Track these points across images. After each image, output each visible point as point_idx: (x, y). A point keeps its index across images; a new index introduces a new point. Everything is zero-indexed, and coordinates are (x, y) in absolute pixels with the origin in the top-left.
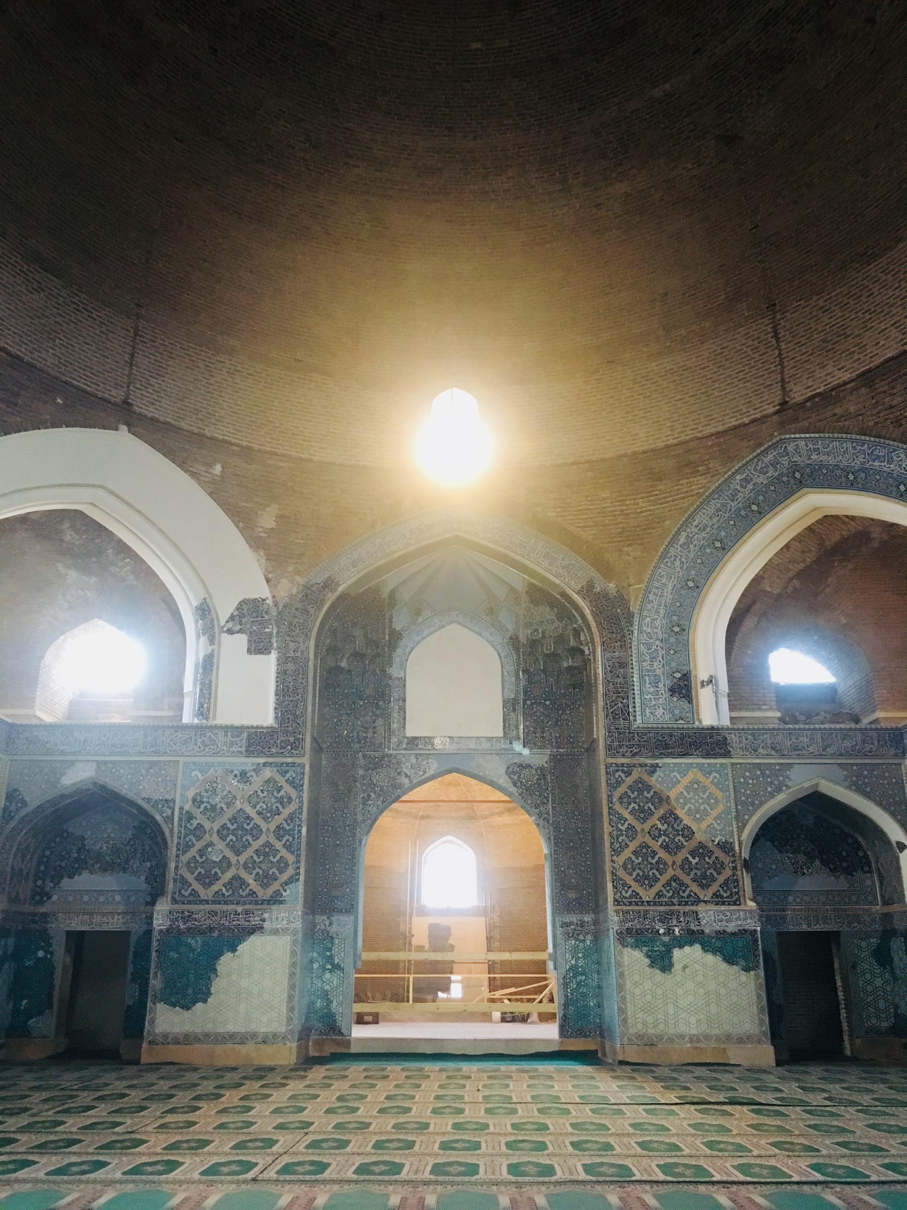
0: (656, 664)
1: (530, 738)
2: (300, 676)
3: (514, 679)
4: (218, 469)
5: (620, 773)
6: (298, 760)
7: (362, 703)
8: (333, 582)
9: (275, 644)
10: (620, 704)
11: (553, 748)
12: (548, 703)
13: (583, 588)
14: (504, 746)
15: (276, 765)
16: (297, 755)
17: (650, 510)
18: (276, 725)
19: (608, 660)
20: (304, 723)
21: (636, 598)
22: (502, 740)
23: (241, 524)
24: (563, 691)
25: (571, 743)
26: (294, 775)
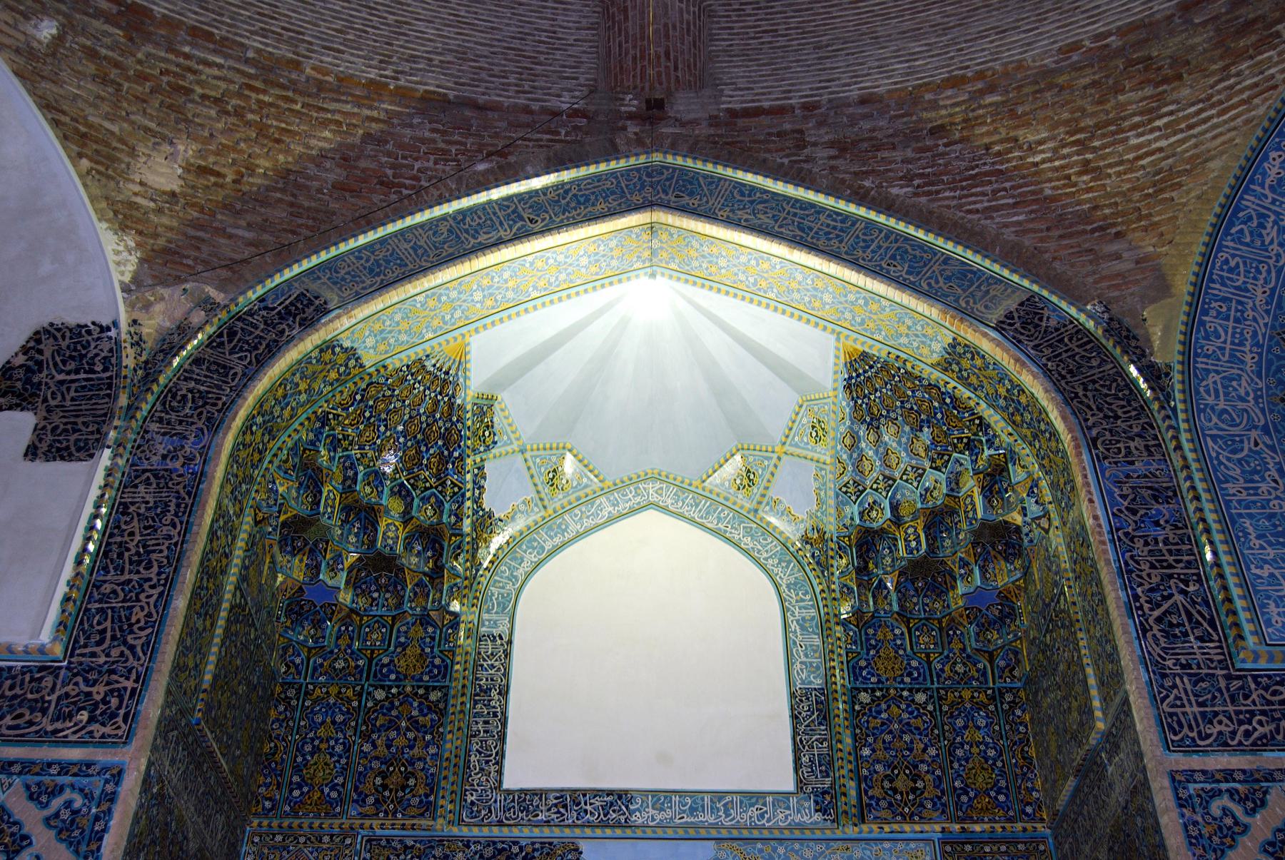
0: (1264, 487)
1: (876, 792)
2: (169, 517)
3: (817, 641)
4: (47, 30)
5: (1225, 801)
6: (102, 756)
7: (380, 695)
8: (311, 303)
9: (112, 434)
10: (1178, 598)
11: (950, 820)
12: (920, 698)
13: (1009, 316)
14: (798, 818)
15: (27, 767)
16: (103, 742)
17: (1161, 150)
18: (58, 650)
19: (1119, 483)
20: (151, 648)
21: (1167, 330)
22: (793, 801)
23: (85, 163)
24: (960, 668)
25: (999, 805)
26: (78, 802)
